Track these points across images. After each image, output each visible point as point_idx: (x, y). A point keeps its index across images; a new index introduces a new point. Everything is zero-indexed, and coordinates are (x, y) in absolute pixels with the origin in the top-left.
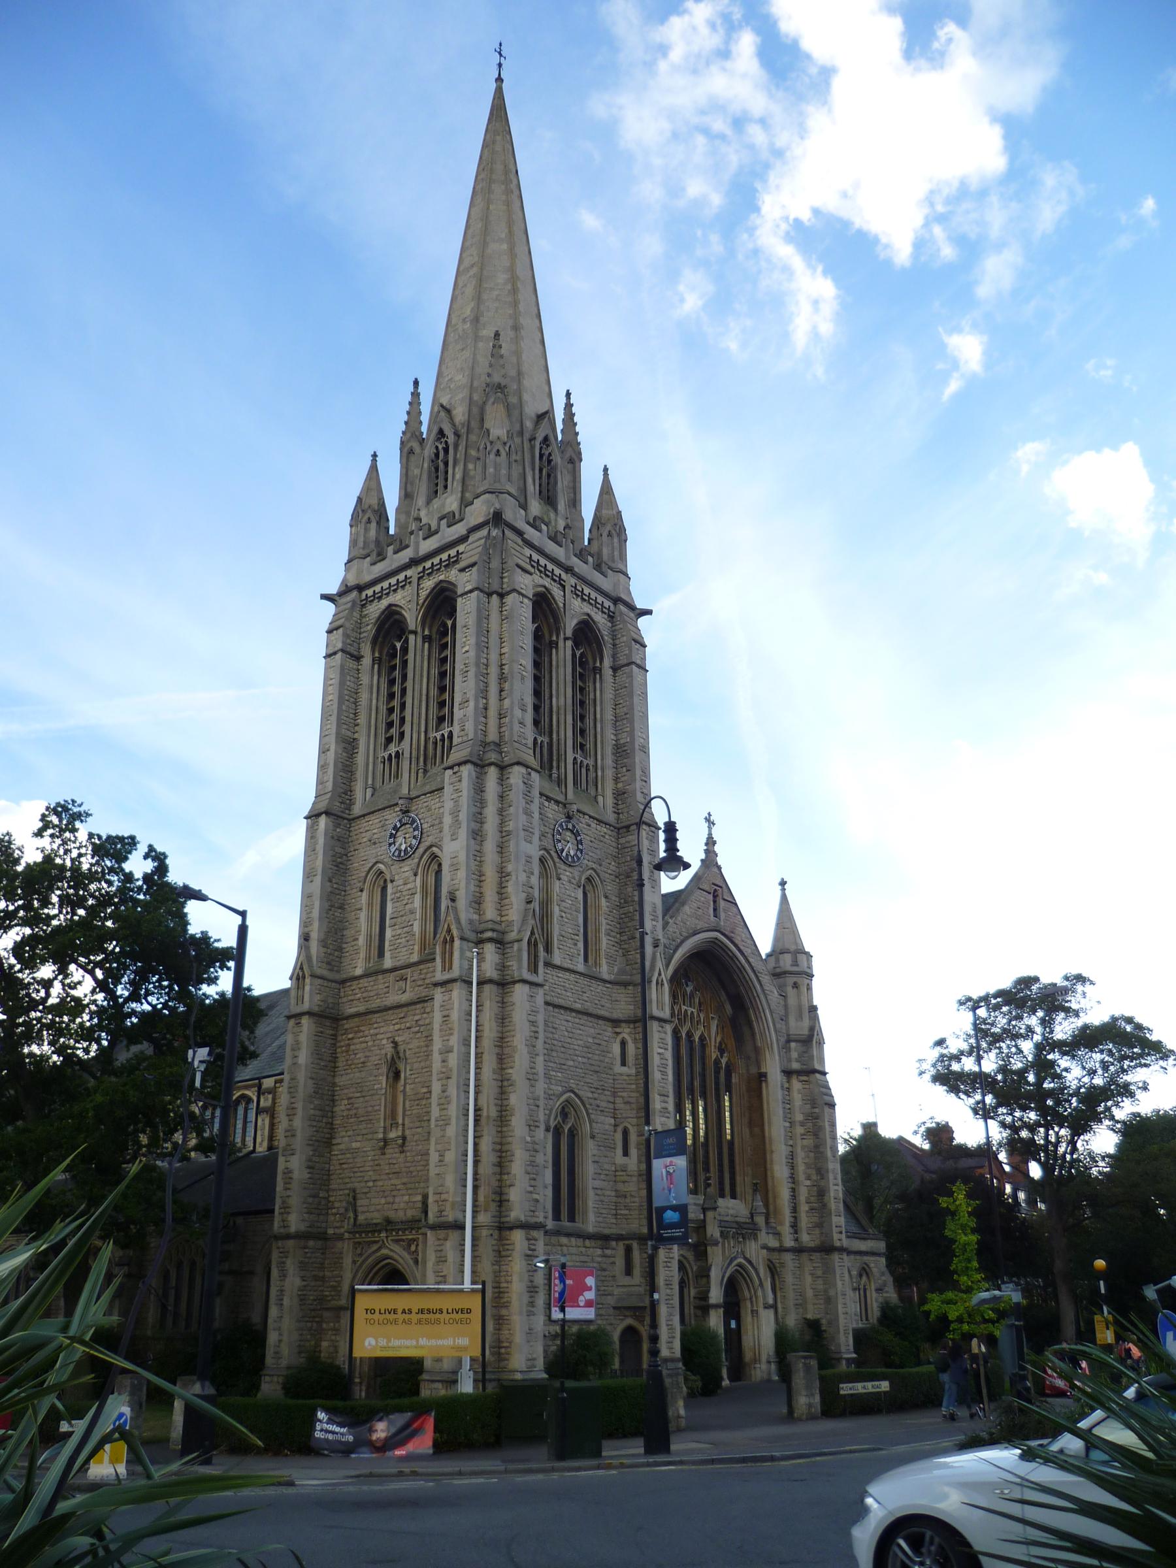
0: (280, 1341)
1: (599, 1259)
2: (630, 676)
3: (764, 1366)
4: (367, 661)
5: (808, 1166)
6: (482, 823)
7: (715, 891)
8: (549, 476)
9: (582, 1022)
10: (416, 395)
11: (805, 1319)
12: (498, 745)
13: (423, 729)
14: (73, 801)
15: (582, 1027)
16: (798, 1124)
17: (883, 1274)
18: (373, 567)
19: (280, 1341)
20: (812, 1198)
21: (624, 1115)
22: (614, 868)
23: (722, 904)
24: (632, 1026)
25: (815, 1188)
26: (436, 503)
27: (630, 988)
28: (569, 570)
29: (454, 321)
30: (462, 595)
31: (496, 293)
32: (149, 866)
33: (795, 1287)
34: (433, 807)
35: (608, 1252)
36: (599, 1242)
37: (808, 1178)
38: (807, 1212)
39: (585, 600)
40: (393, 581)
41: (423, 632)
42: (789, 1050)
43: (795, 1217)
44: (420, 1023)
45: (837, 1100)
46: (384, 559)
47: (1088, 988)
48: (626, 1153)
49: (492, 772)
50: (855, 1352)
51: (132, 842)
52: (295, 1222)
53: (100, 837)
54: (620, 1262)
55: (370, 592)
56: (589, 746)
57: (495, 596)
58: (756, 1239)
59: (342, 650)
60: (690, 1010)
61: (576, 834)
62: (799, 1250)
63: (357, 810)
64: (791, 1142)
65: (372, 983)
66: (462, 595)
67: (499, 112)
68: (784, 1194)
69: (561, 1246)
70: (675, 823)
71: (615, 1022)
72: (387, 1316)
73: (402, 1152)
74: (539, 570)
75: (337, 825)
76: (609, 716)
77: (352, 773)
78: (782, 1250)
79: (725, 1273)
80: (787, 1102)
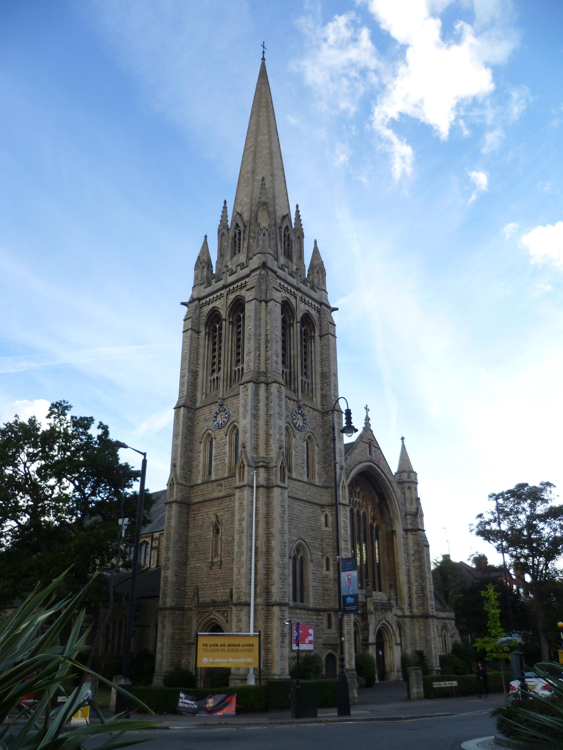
0: (162, 659)
1: (315, 621)
2: (328, 340)
3: (396, 673)
4: (203, 334)
5: (416, 576)
6: (258, 411)
7: (370, 442)
8: (288, 245)
9: (306, 506)
10: (225, 208)
11: (415, 650)
12: (265, 373)
13: (229, 366)
14: (64, 401)
15: (306, 508)
16: (411, 555)
17: (454, 629)
18: (206, 289)
19: (162, 659)
21: (327, 551)
22: (321, 432)
23: (373, 449)
24: (330, 508)
25: (420, 587)
26: (235, 259)
27: (329, 489)
28: (298, 289)
29: (243, 173)
30: (248, 302)
31: (262, 159)
32: (100, 432)
33: (411, 635)
34: (234, 403)
35: (320, 617)
36: (315, 613)
37: (417, 582)
38: (416, 598)
39: (306, 304)
40: (215, 296)
41: (229, 320)
42: (406, 519)
43: (410, 601)
44: (229, 506)
45: (430, 544)
46: (210, 285)
47: (552, 489)
48: (328, 569)
49: (263, 386)
50: (440, 667)
51: (91, 420)
52: (169, 602)
53: (76, 418)
54: (325, 622)
55: (204, 301)
56: (309, 373)
57: (263, 302)
58: (391, 611)
59: (191, 329)
60: (358, 500)
61: (303, 416)
62: (412, 617)
63: (198, 404)
64: (408, 564)
65: (206, 487)
66: (248, 302)
67: (263, 74)
68: (405, 589)
69: (297, 614)
70: (350, 410)
71: (322, 506)
72: (213, 647)
73: (220, 568)
74: (284, 289)
75: (189, 412)
76: (318, 359)
77: (196, 387)
78: (404, 616)
79: (376, 627)
80: (406, 544)
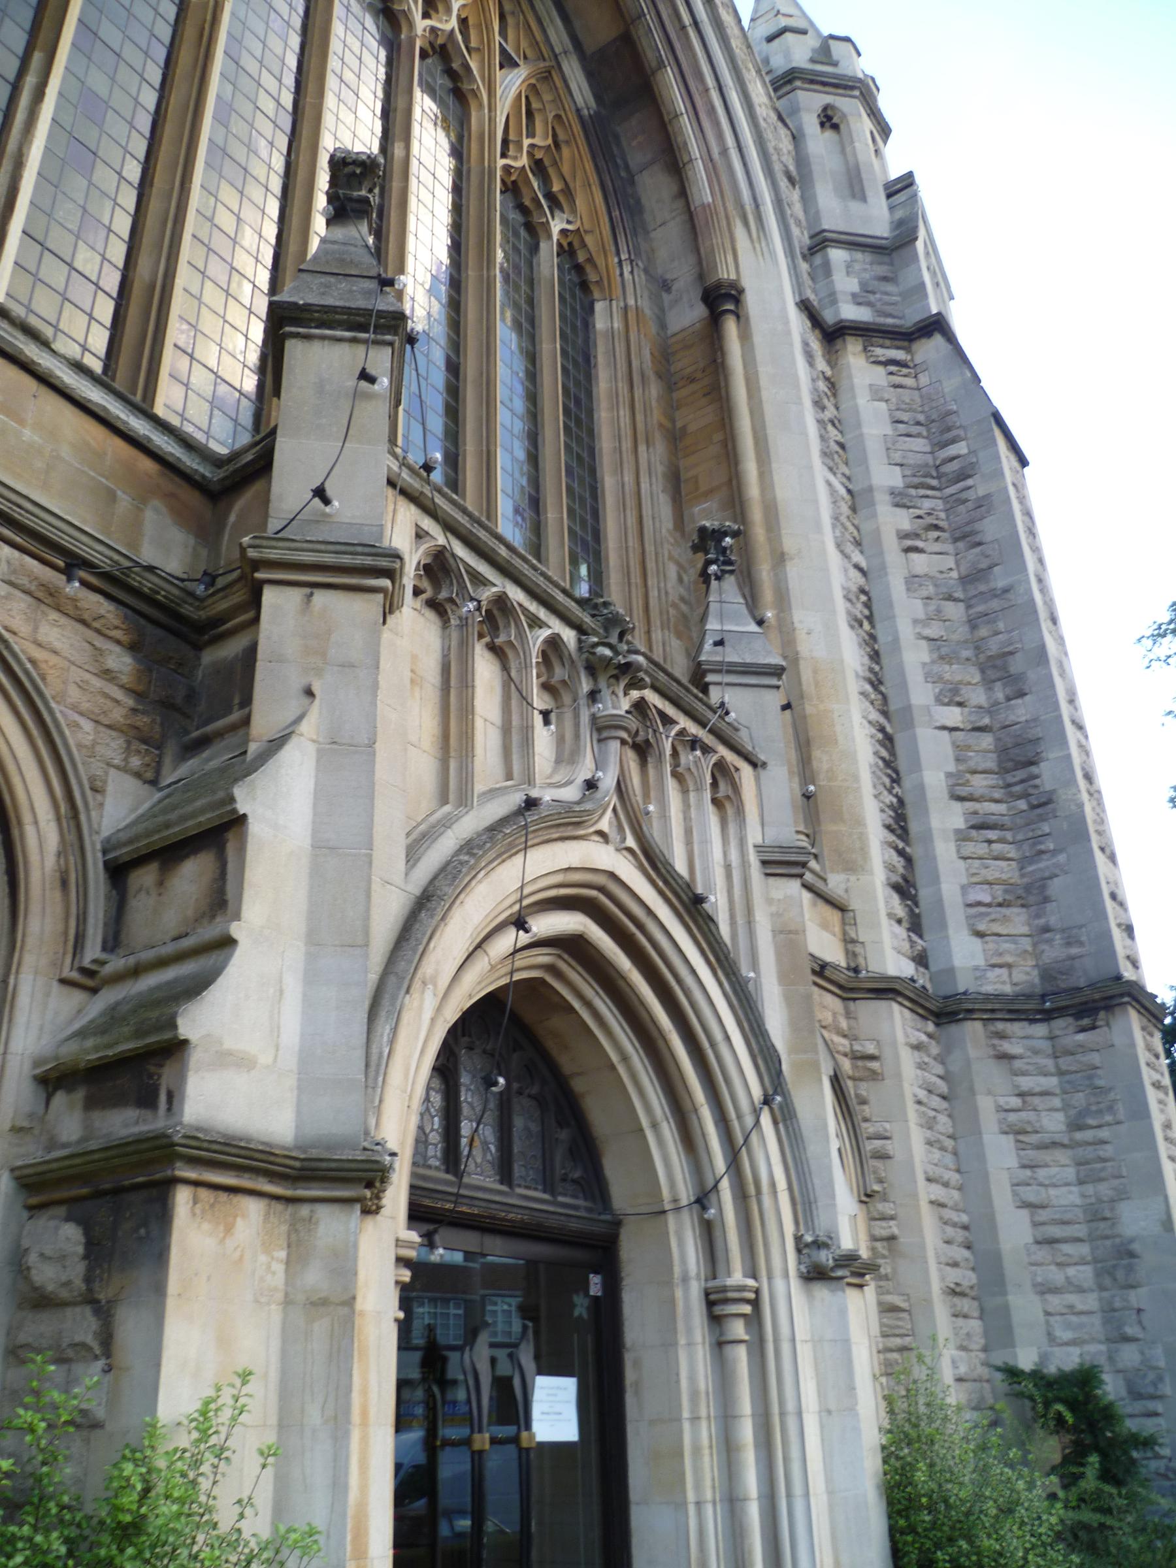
20: (979, 783)
25: (987, 741)
38: (961, 837)
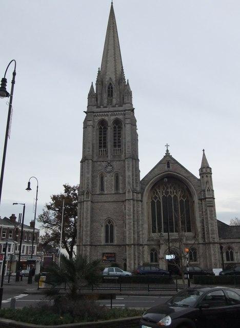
28: (108, 112)
62: (204, 244)
68: (199, 230)
71: (123, 202)
